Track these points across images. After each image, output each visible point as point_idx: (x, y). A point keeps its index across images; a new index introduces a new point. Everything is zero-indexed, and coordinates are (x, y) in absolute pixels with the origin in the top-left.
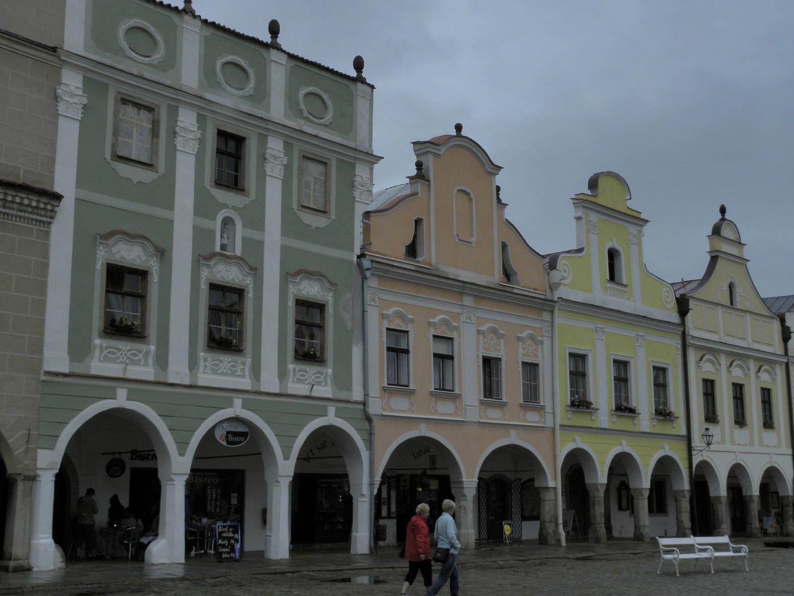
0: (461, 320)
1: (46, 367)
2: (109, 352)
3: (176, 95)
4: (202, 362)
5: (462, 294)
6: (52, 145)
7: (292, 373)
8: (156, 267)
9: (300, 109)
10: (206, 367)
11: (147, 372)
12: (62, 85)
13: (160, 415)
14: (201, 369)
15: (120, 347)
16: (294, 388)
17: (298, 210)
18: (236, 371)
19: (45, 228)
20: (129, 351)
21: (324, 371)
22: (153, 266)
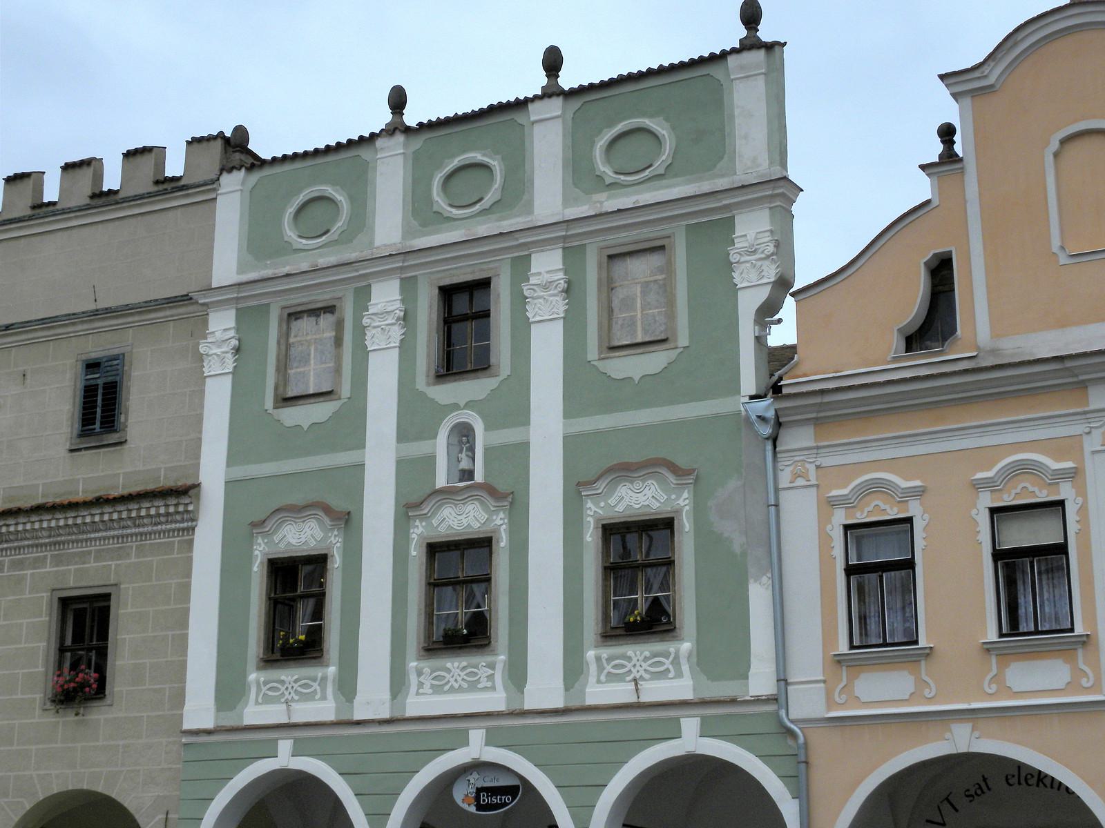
0: (1088, 448)
1: (186, 726)
2: (269, 689)
3: (357, 271)
4: (413, 679)
5: (1083, 386)
6: (197, 422)
7: (593, 668)
8: (338, 545)
9: (598, 176)
10: (421, 685)
11: (324, 709)
12: (208, 336)
13: (340, 774)
14: (413, 689)
15: (283, 678)
16: (598, 692)
17: (600, 359)
18: (478, 681)
19: (190, 535)
20: (296, 681)
21: (672, 650)
22: (335, 545)
